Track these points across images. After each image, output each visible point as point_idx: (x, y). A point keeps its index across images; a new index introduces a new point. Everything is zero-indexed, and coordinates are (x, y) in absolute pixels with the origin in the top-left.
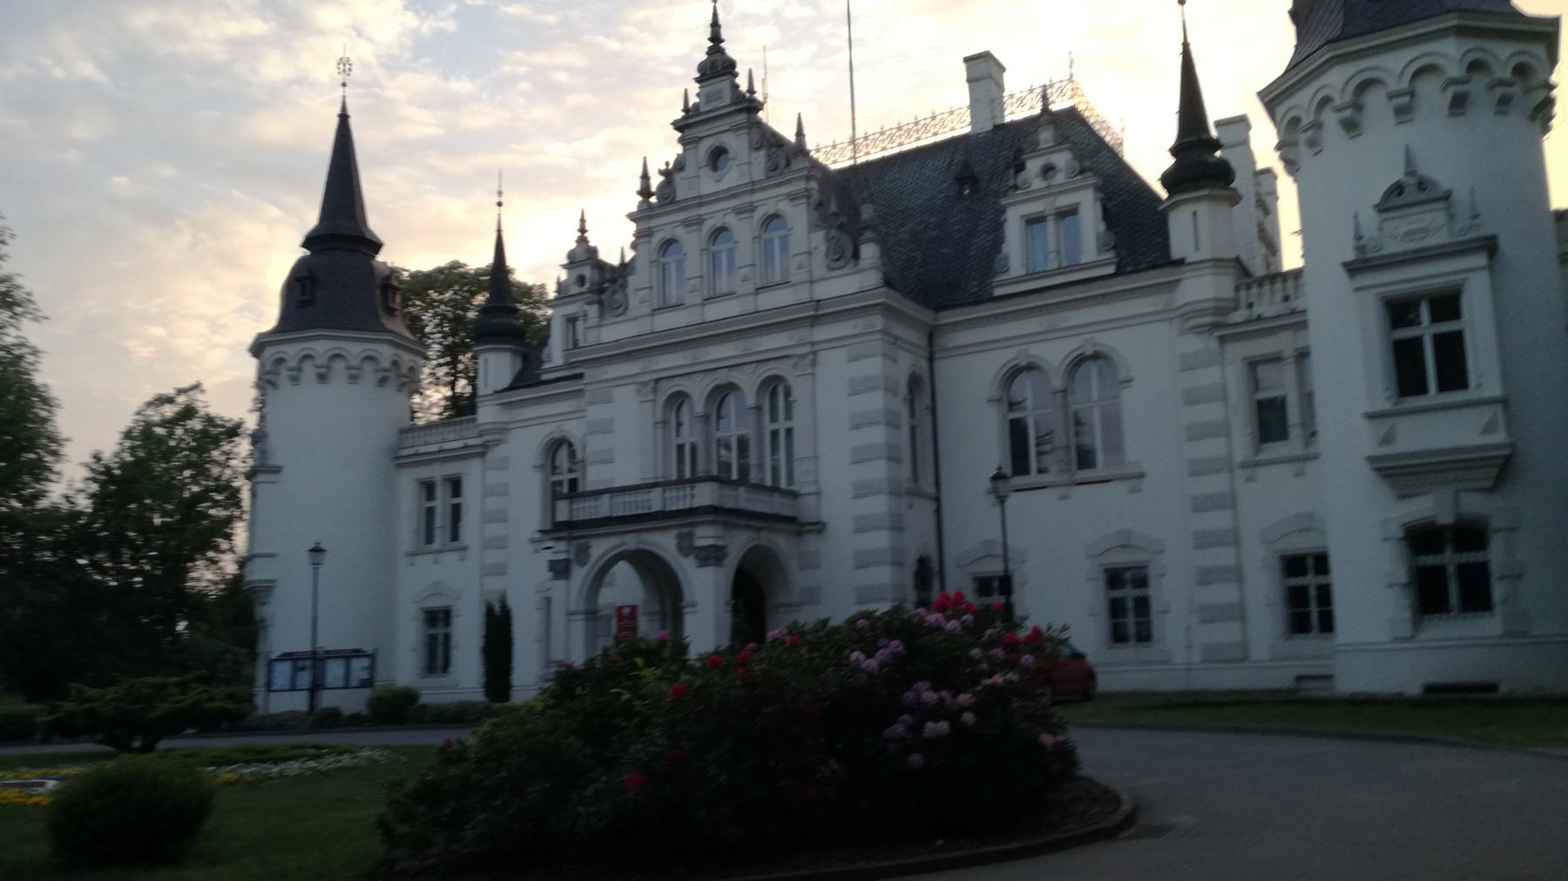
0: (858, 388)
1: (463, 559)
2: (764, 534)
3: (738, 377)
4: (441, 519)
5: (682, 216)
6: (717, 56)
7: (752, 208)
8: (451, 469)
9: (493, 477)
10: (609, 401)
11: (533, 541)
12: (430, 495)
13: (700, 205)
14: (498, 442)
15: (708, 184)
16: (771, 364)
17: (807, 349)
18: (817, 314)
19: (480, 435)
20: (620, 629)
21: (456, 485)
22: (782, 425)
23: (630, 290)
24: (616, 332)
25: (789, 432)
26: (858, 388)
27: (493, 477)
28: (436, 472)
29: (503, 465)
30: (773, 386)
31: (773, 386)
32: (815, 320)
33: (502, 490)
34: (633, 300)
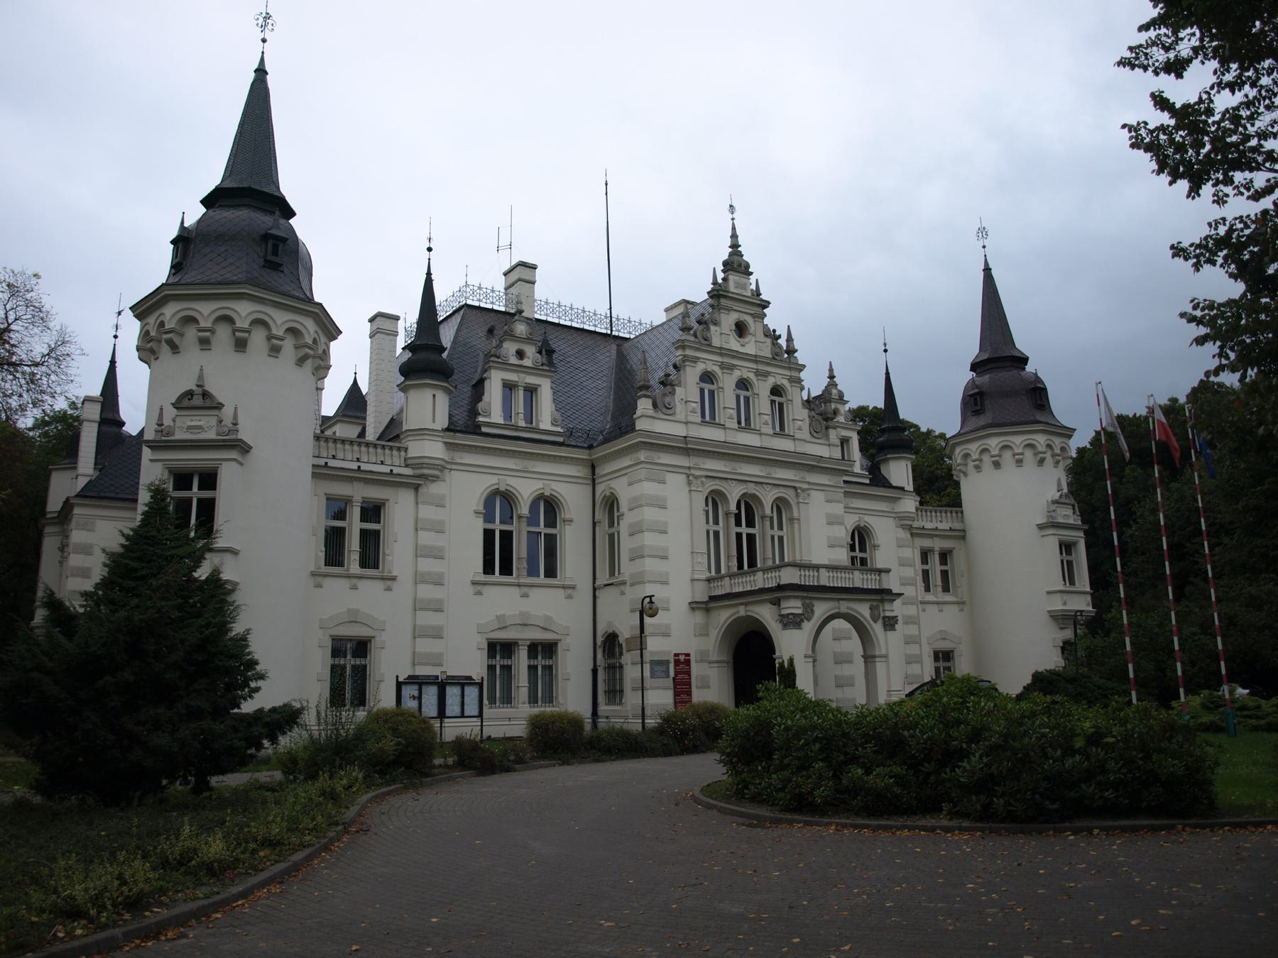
0: (833, 521)
1: (389, 589)
2: (750, 608)
4: (353, 543)
6: (736, 258)
8: (375, 493)
9: (427, 512)
11: (474, 583)
12: (340, 515)
13: (734, 357)
14: (435, 479)
15: (734, 344)
17: (805, 486)
19: (407, 466)
20: (677, 673)
21: (373, 511)
22: (776, 533)
24: (662, 427)
25: (781, 539)
30: (781, 505)
31: (781, 505)
33: (439, 528)
34: (679, 407)
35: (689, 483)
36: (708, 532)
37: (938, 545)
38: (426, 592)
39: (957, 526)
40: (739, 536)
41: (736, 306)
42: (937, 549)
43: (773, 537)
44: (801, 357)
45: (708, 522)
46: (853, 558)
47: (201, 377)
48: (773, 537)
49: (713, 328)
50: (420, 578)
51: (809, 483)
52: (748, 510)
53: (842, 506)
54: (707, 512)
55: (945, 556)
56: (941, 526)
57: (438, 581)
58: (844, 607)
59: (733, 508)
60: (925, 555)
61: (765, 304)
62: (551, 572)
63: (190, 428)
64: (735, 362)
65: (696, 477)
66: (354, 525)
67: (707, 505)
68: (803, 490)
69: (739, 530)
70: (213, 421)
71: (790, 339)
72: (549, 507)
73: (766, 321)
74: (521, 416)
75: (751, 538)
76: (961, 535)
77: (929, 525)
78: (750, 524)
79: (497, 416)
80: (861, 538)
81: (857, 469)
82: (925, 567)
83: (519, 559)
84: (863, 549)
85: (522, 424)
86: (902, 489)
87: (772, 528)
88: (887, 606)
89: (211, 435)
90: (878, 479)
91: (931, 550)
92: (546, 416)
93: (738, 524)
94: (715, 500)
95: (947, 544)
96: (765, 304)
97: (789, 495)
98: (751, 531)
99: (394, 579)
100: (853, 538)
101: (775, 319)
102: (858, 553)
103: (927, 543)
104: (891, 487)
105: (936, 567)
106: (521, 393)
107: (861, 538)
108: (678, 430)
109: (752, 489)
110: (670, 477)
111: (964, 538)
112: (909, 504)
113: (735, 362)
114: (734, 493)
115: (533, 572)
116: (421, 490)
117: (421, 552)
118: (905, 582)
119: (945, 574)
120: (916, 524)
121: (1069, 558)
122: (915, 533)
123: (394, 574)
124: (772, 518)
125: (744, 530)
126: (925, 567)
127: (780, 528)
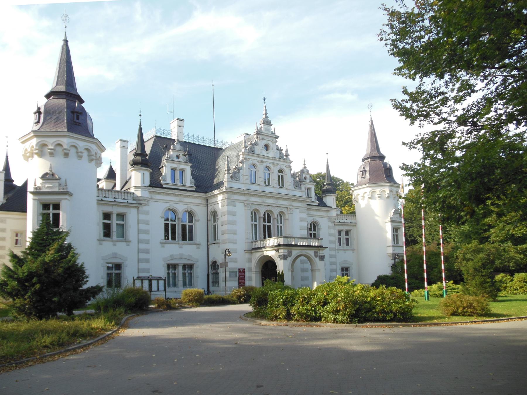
0: (302, 220)
1: (128, 245)
3: (273, 209)
4: (114, 229)
5: (258, 159)
7: (277, 164)
9: (142, 217)
10: (235, 206)
11: (161, 243)
13: (264, 158)
15: (264, 153)
16: (256, 206)
18: (296, 199)
21: (122, 216)
22: (279, 225)
23: (240, 174)
25: (281, 227)
26: (302, 220)
27: (142, 217)
28: (115, 210)
29: (147, 213)
30: (281, 214)
31: (281, 214)
32: (294, 200)
33: (147, 223)
34: (241, 177)
35: (245, 206)
36: (252, 224)
37: (345, 228)
38: (142, 246)
39: (353, 221)
40: (264, 226)
41: (265, 138)
42: (345, 230)
43: (278, 226)
44: (291, 158)
45: (252, 221)
46: (311, 234)
47: (50, 168)
48: (278, 226)
49: (255, 147)
50: (139, 241)
51: (293, 206)
52: (268, 217)
53: (306, 214)
54: (252, 217)
55: (347, 233)
56: (346, 221)
57: (147, 242)
58: (304, 252)
59: (262, 215)
60: (339, 233)
61: (277, 137)
62: (191, 239)
63: (48, 187)
64: (264, 160)
65: (248, 204)
66: (114, 222)
67: (252, 214)
68: (291, 209)
69: (264, 224)
70: (57, 184)
71: (287, 151)
72: (191, 215)
73: (277, 144)
74: (179, 181)
75: (269, 227)
76: (355, 224)
77: (341, 221)
78: (269, 221)
79: (169, 181)
80: (314, 226)
81: (313, 200)
82: (340, 237)
83: (178, 234)
84: (315, 230)
85: (179, 183)
86: (331, 207)
87: (278, 223)
88: (321, 252)
89: (56, 190)
90: (322, 204)
91: (342, 230)
92: (189, 180)
93: (264, 221)
94: (255, 213)
95: (348, 228)
96: (277, 137)
97: (285, 210)
98: (269, 224)
99: (130, 242)
100: (311, 226)
101: (280, 143)
102: (312, 232)
103: (341, 228)
104: (327, 206)
105: (343, 236)
106: (178, 172)
107: (314, 226)
108: (242, 186)
109: (269, 208)
110: (237, 204)
111: (355, 225)
112: (334, 213)
113: (264, 160)
114: (262, 210)
115: (184, 239)
116: (140, 209)
117: (139, 232)
118: (331, 242)
119: (347, 240)
120: (336, 221)
121: (397, 234)
122: (335, 224)
123: (130, 240)
124: (277, 220)
125: (267, 224)
126: (340, 237)
127: (281, 223)
